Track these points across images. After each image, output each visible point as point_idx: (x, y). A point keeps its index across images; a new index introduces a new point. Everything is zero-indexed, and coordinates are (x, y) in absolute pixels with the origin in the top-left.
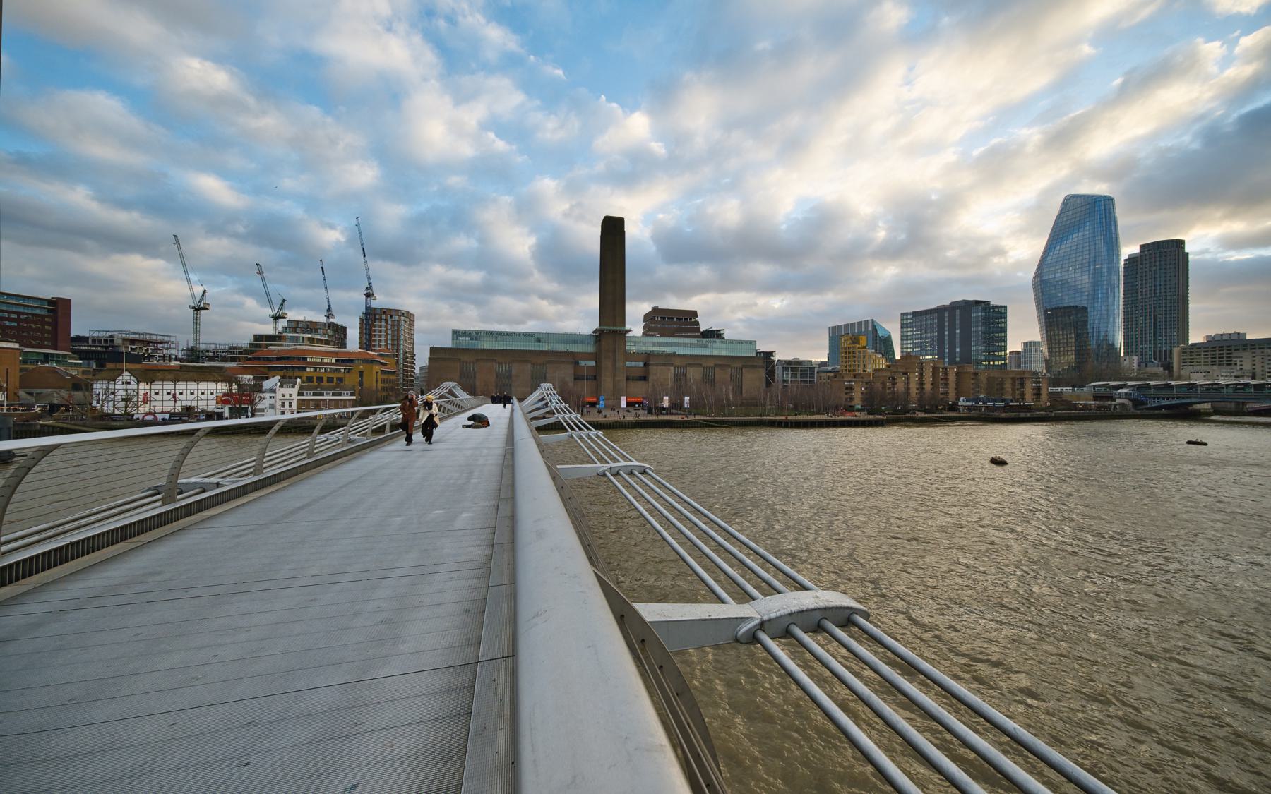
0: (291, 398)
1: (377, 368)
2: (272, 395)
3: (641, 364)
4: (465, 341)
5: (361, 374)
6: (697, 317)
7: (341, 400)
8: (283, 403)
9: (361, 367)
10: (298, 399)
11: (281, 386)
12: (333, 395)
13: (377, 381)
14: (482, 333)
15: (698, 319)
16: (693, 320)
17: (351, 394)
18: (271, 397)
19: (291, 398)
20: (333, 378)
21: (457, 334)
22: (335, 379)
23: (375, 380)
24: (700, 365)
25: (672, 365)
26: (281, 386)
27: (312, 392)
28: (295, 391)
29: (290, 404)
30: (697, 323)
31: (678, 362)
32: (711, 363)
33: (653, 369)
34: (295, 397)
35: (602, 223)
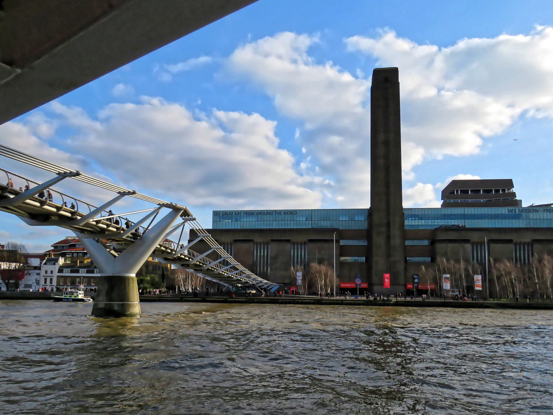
0: (52, 275)
2: (38, 271)
3: (426, 243)
6: (513, 187)
8: (46, 280)
10: (57, 276)
12: (88, 272)
14: (242, 214)
15: (514, 190)
16: (506, 191)
18: (37, 274)
19: (52, 275)
24: (510, 241)
25: (467, 241)
27: (69, 270)
29: (51, 280)
30: (514, 194)
31: (475, 237)
32: (527, 238)
33: (439, 247)
34: (56, 274)
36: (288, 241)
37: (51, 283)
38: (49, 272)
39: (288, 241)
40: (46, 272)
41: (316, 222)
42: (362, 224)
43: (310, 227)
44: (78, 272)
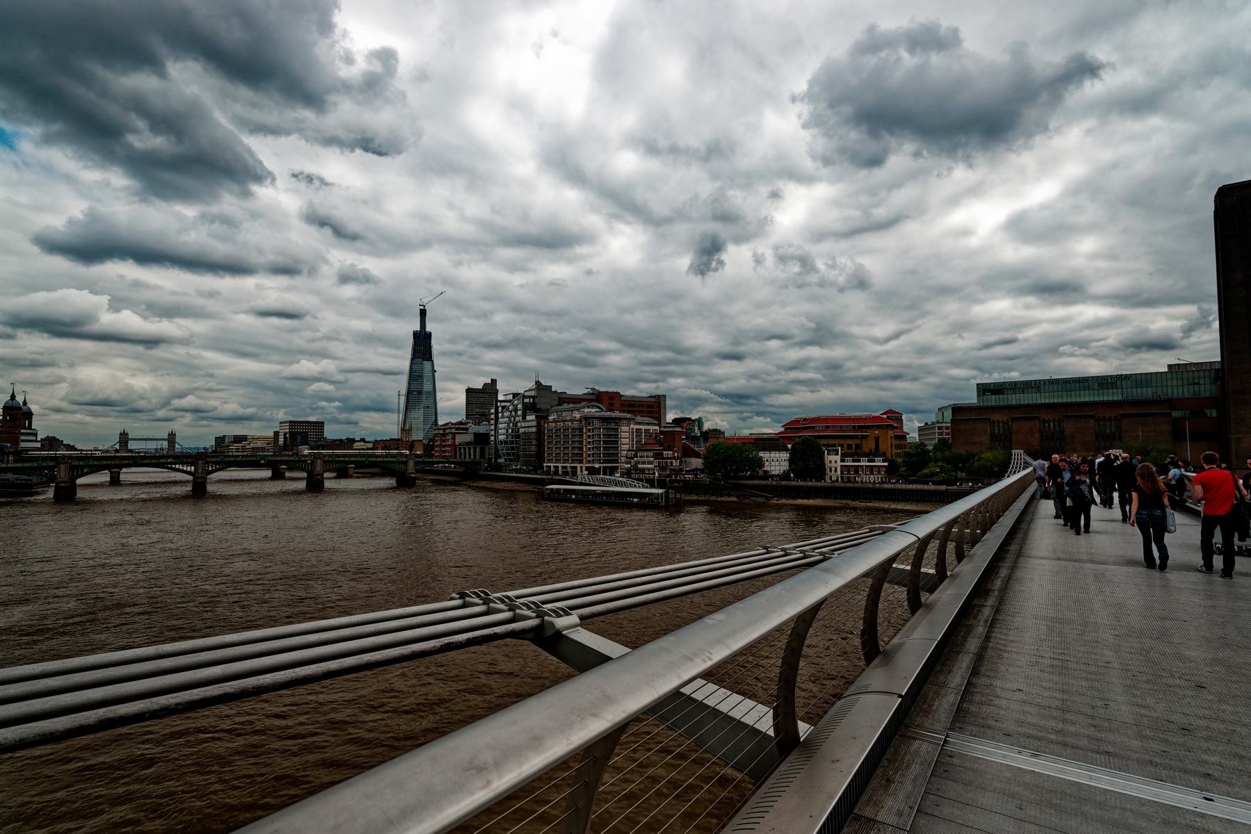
1: (891, 433)
4: (993, 400)
5: (877, 439)
7: (876, 466)
9: (877, 432)
11: (828, 454)
12: (869, 461)
13: (892, 447)
17: (884, 461)
20: (851, 445)
21: (983, 389)
22: (854, 446)
23: (890, 446)
26: (828, 454)
28: (838, 458)
29: (836, 469)
34: (839, 464)
35: (1215, 197)
36: (1091, 417)
37: (836, 471)
38: (833, 462)
39: (1091, 417)
40: (830, 462)
41: (1130, 390)
42: (1207, 389)
43: (1120, 398)
44: (859, 461)
